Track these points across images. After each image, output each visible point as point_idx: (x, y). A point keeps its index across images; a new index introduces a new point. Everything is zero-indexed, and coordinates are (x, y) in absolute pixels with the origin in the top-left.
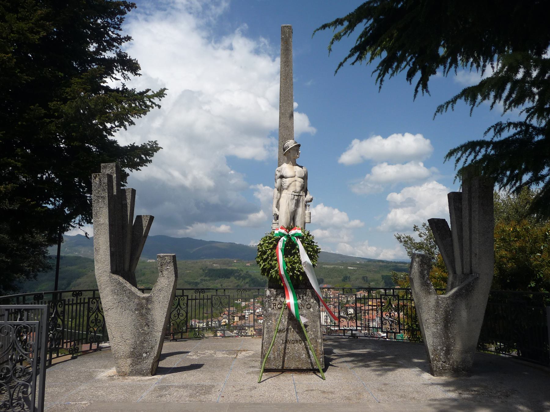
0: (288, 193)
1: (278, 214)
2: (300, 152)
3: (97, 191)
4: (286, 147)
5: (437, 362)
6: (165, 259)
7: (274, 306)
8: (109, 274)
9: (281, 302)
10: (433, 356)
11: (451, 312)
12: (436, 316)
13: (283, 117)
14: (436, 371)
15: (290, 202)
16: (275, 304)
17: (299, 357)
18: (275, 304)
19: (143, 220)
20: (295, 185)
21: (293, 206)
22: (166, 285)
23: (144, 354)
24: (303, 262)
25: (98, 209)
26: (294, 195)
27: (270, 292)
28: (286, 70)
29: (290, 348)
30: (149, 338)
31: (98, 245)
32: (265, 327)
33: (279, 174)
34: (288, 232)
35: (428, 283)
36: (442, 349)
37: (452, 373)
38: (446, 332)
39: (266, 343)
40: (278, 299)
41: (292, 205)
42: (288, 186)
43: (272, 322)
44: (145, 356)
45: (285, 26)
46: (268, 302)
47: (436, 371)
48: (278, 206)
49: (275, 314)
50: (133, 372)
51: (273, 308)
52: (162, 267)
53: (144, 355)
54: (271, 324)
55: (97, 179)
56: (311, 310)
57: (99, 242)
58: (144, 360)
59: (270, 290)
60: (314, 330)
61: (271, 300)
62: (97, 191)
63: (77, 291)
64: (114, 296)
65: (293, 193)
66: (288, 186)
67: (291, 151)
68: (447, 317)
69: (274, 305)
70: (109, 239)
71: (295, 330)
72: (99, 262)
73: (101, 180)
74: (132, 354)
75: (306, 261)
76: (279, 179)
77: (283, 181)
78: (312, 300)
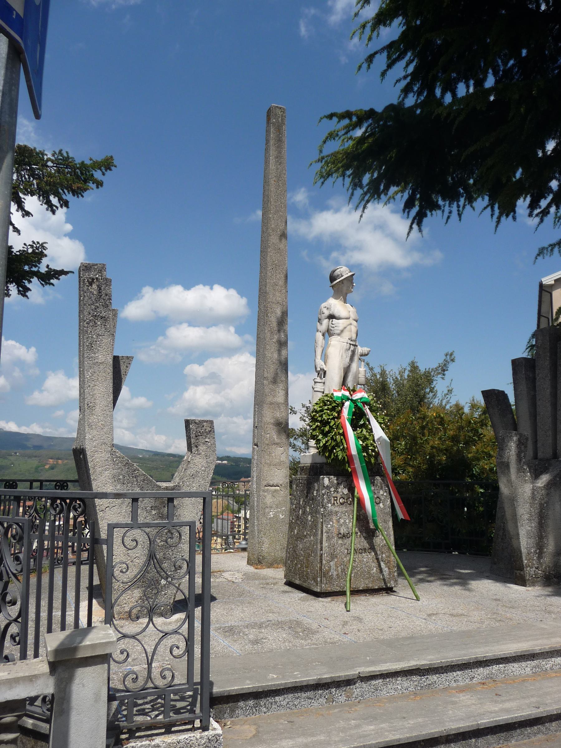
0: (342, 340)
1: (325, 369)
2: (354, 285)
3: (93, 307)
4: (338, 275)
5: (530, 568)
6: (203, 426)
7: (334, 500)
8: (110, 449)
9: (343, 495)
10: (526, 562)
11: (545, 505)
12: (530, 510)
13: (273, 234)
14: (528, 579)
15: (343, 353)
16: (337, 497)
17: (369, 572)
18: (337, 497)
19: (121, 363)
20: (351, 331)
21: (348, 360)
22: (203, 468)
23: (163, 580)
24: (376, 438)
25: (94, 336)
26: (350, 344)
27: (329, 481)
28: (277, 169)
29: (357, 560)
30: (173, 554)
31: (93, 399)
32: (324, 532)
33: (327, 313)
34: (351, 395)
35: (524, 469)
36: (535, 551)
37: (544, 581)
38: (540, 530)
39: (325, 555)
40: (340, 490)
41: (346, 357)
42: (342, 331)
43: (333, 523)
44: (165, 583)
45: (277, 107)
46: (327, 495)
47: (528, 579)
48: (325, 358)
49: (336, 512)
50: (143, 611)
51: (334, 504)
52: (197, 439)
53: (163, 582)
54: (332, 526)
55: (94, 286)
56: (381, 505)
57: (95, 394)
58: (162, 591)
59: (329, 478)
61: (331, 492)
62: (93, 307)
63: (11, 480)
64: (116, 486)
65: (349, 342)
66: (342, 331)
67: (345, 282)
68: (541, 511)
69: (335, 499)
70: (112, 389)
71: (362, 534)
72: (94, 427)
73: (100, 289)
74: (143, 582)
75: (381, 437)
76: (327, 320)
77: (333, 323)
78: (381, 492)
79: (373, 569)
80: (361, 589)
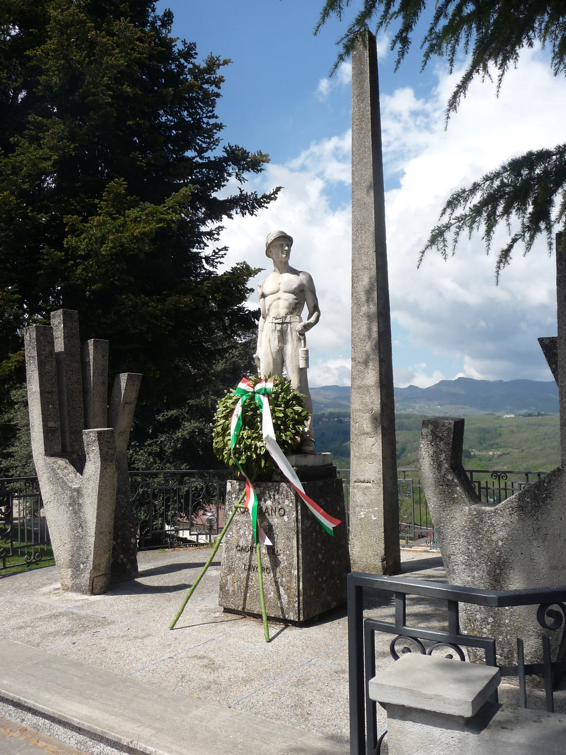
8: (43, 457)
12: (468, 549)
15: (271, 336)
22: (93, 473)
26: (276, 323)
27: (231, 486)
35: (448, 480)
41: (275, 340)
53: (82, 566)
56: (285, 518)
60: (288, 552)
78: (287, 502)
79: (270, 593)
80: (255, 612)
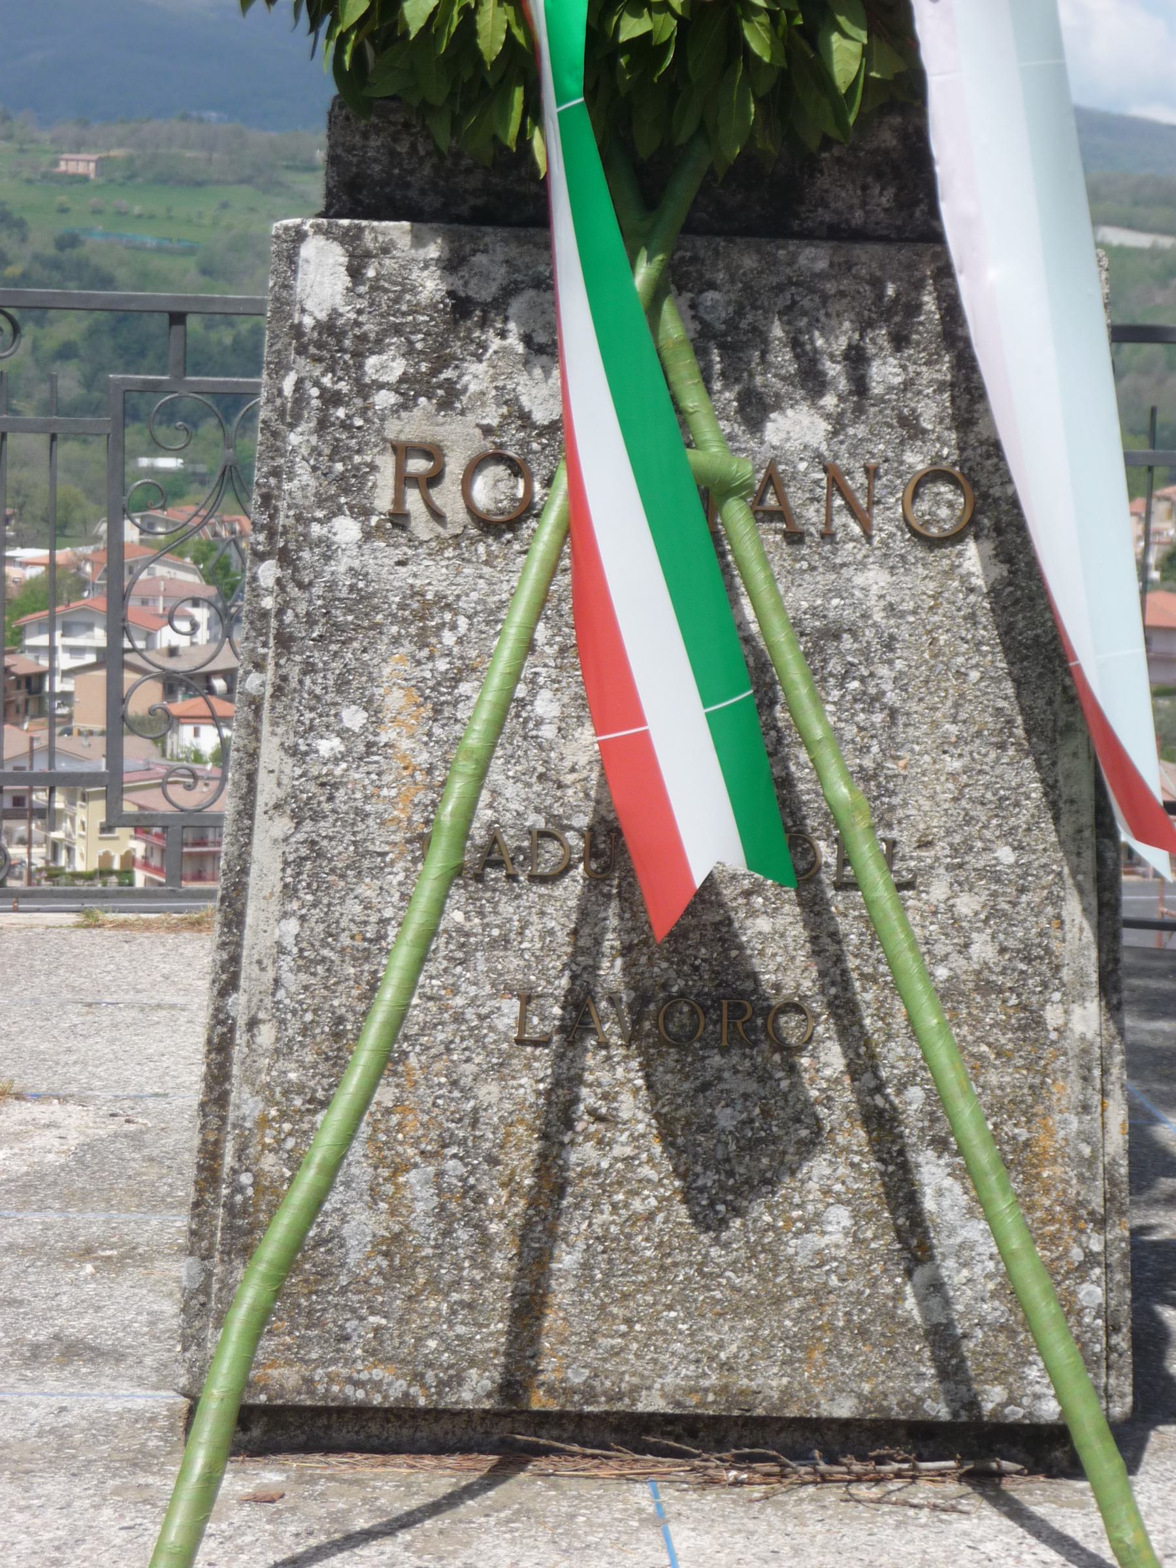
7: (404, 480)
16: (432, 452)
18: (432, 452)
27: (355, 272)
39: (266, 1035)
46: (323, 425)
51: (399, 519)
59: (350, 239)
60: (1006, 855)
61: (364, 390)
69: (418, 465)
79: (813, 1223)
80: (652, 1403)
